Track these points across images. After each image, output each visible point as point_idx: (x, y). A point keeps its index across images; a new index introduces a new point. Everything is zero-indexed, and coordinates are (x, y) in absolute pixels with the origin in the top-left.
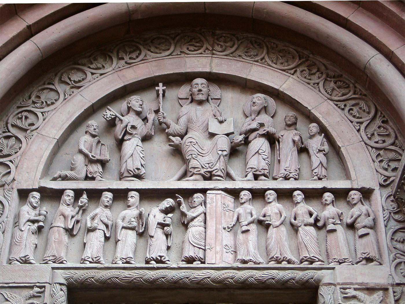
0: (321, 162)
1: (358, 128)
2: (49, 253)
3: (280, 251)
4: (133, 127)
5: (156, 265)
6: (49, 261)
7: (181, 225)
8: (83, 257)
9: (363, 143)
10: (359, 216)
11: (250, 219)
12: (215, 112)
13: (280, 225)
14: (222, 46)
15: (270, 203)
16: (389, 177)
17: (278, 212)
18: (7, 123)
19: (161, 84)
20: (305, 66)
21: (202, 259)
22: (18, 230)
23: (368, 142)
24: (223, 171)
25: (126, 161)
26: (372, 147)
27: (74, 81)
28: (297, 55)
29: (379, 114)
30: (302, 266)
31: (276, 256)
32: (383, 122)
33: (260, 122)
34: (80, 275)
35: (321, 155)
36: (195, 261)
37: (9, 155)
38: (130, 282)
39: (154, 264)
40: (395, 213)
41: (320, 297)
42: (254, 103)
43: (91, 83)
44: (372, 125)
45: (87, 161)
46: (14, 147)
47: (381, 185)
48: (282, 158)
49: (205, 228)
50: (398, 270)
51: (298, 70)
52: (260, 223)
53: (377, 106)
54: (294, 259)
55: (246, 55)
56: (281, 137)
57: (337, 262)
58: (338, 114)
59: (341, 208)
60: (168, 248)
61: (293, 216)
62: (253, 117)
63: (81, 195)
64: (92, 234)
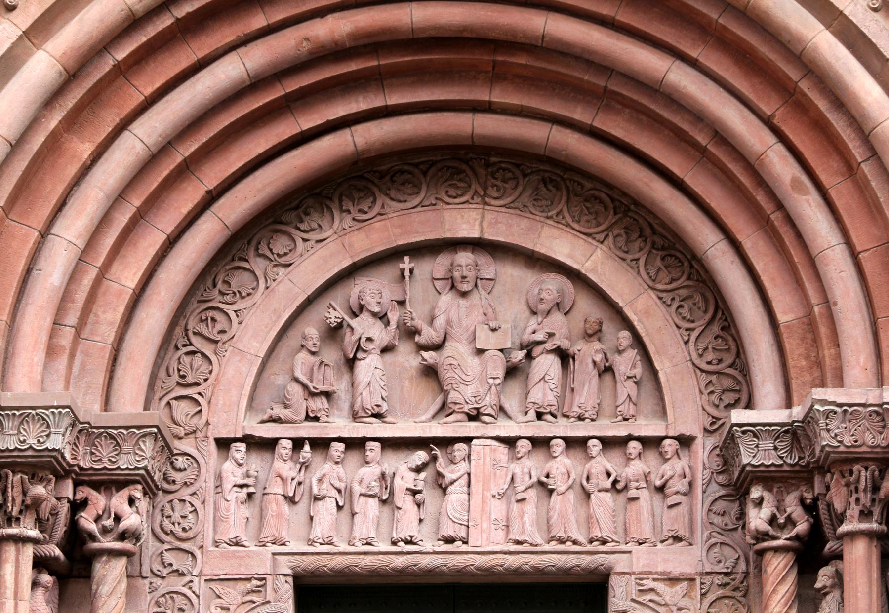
0: (629, 395)
1: (686, 338)
2: (267, 532)
4: (369, 339)
7: (437, 487)
8: (311, 538)
9: (689, 364)
10: (671, 477)
11: (528, 482)
12: (486, 309)
13: (567, 490)
14: (498, 190)
15: (555, 457)
16: (719, 419)
17: (566, 471)
18: (186, 330)
20: (621, 228)
22: (223, 500)
23: (697, 362)
24: (495, 407)
25: (361, 394)
27: (278, 255)
28: (612, 206)
30: (589, 548)
33: (548, 331)
34: (309, 563)
35: (630, 384)
37: (197, 384)
38: (373, 571)
40: (720, 473)
41: (610, 589)
42: (542, 299)
43: (303, 258)
44: (707, 332)
45: (307, 393)
46: (201, 370)
47: (705, 430)
48: (576, 385)
49: (469, 494)
50: (712, 553)
51: (611, 234)
53: (719, 301)
54: (582, 539)
55: (534, 205)
56: (577, 352)
58: (661, 314)
60: (421, 521)
61: (585, 476)
63: (302, 447)
64: (320, 503)
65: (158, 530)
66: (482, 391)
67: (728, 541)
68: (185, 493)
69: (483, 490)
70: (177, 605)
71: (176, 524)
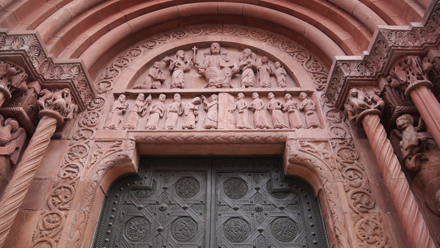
0: (283, 79)
1: (302, 64)
3: (262, 122)
4: (179, 64)
5: (188, 130)
6: (126, 128)
8: (146, 126)
10: (307, 104)
11: (244, 106)
14: (227, 31)
15: (255, 98)
19: (195, 47)
21: (216, 127)
23: (308, 70)
24: (228, 84)
25: (174, 80)
26: (310, 72)
27: (150, 46)
29: (312, 58)
31: (260, 124)
32: (315, 61)
34: (143, 135)
35: (282, 76)
36: (211, 128)
37: (111, 78)
38: (172, 139)
39: (187, 129)
45: (153, 80)
48: (261, 77)
50: (333, 131)
51: (267, 40)
52: (250, 109)
54: (270, 126)
57: (296, 128)
59: (295, 101)
60: (196, 122)
61: (268, 106)
62: (244, 59)
64: (152, 115)
65: (81, 123)
66: (223, 79)
67: (339, 126)
68: (96, 111)
69: (224, 109)
70: (80, 151)
71: (89, 121)
